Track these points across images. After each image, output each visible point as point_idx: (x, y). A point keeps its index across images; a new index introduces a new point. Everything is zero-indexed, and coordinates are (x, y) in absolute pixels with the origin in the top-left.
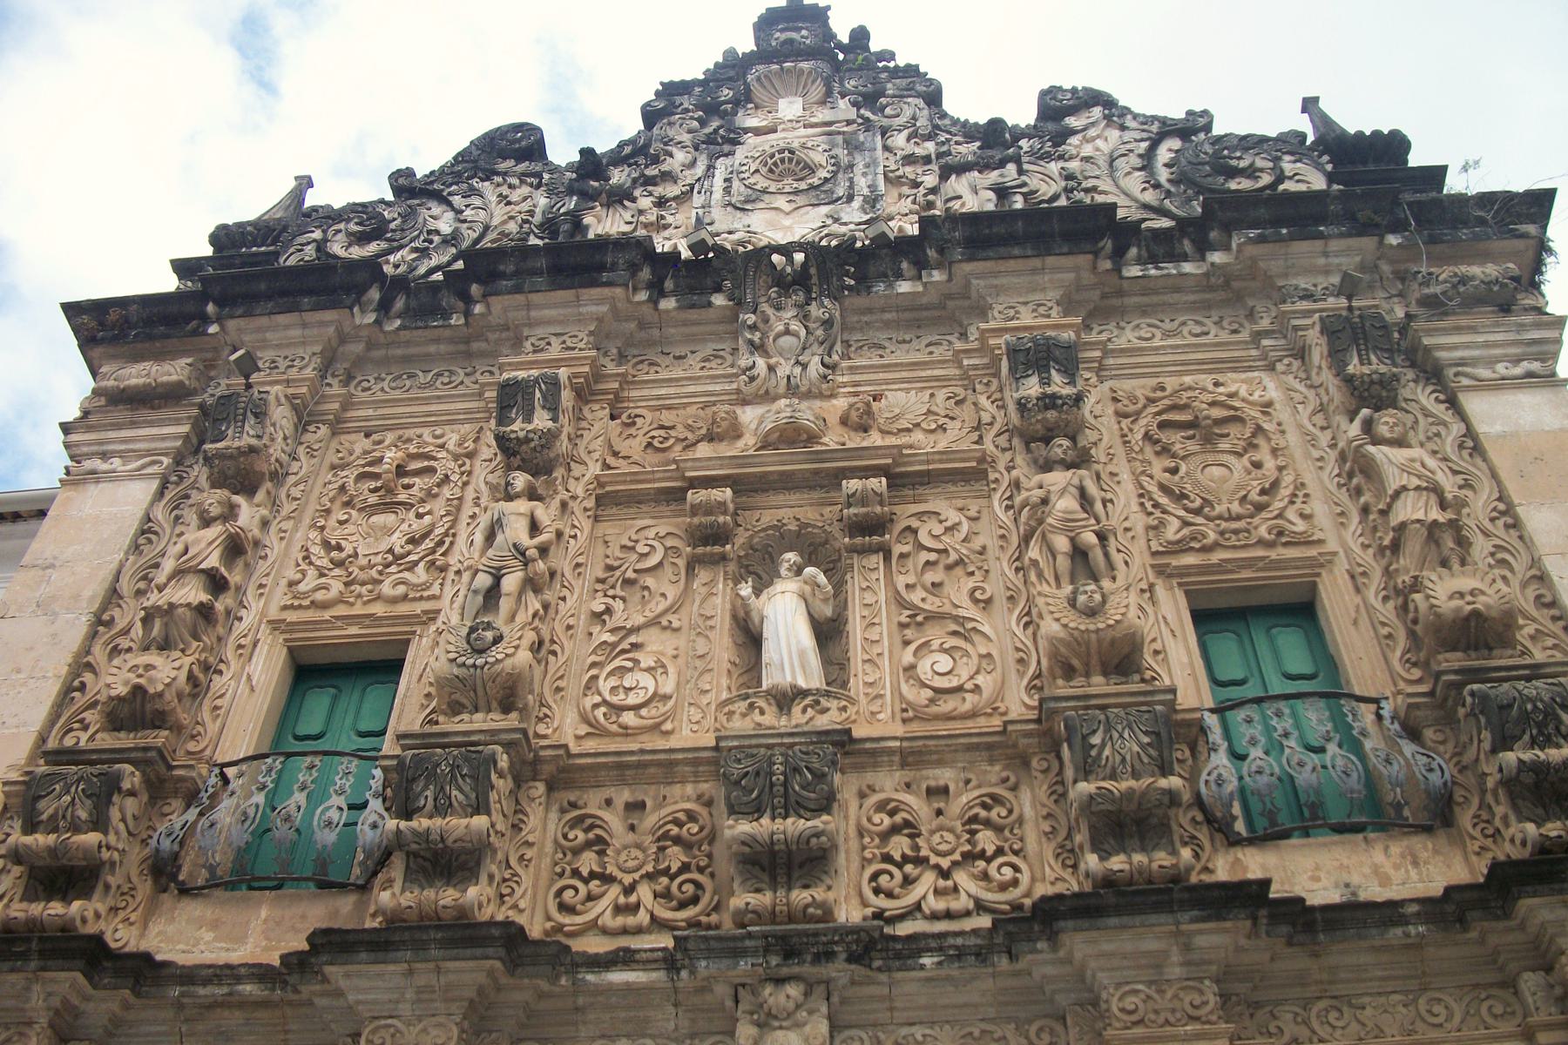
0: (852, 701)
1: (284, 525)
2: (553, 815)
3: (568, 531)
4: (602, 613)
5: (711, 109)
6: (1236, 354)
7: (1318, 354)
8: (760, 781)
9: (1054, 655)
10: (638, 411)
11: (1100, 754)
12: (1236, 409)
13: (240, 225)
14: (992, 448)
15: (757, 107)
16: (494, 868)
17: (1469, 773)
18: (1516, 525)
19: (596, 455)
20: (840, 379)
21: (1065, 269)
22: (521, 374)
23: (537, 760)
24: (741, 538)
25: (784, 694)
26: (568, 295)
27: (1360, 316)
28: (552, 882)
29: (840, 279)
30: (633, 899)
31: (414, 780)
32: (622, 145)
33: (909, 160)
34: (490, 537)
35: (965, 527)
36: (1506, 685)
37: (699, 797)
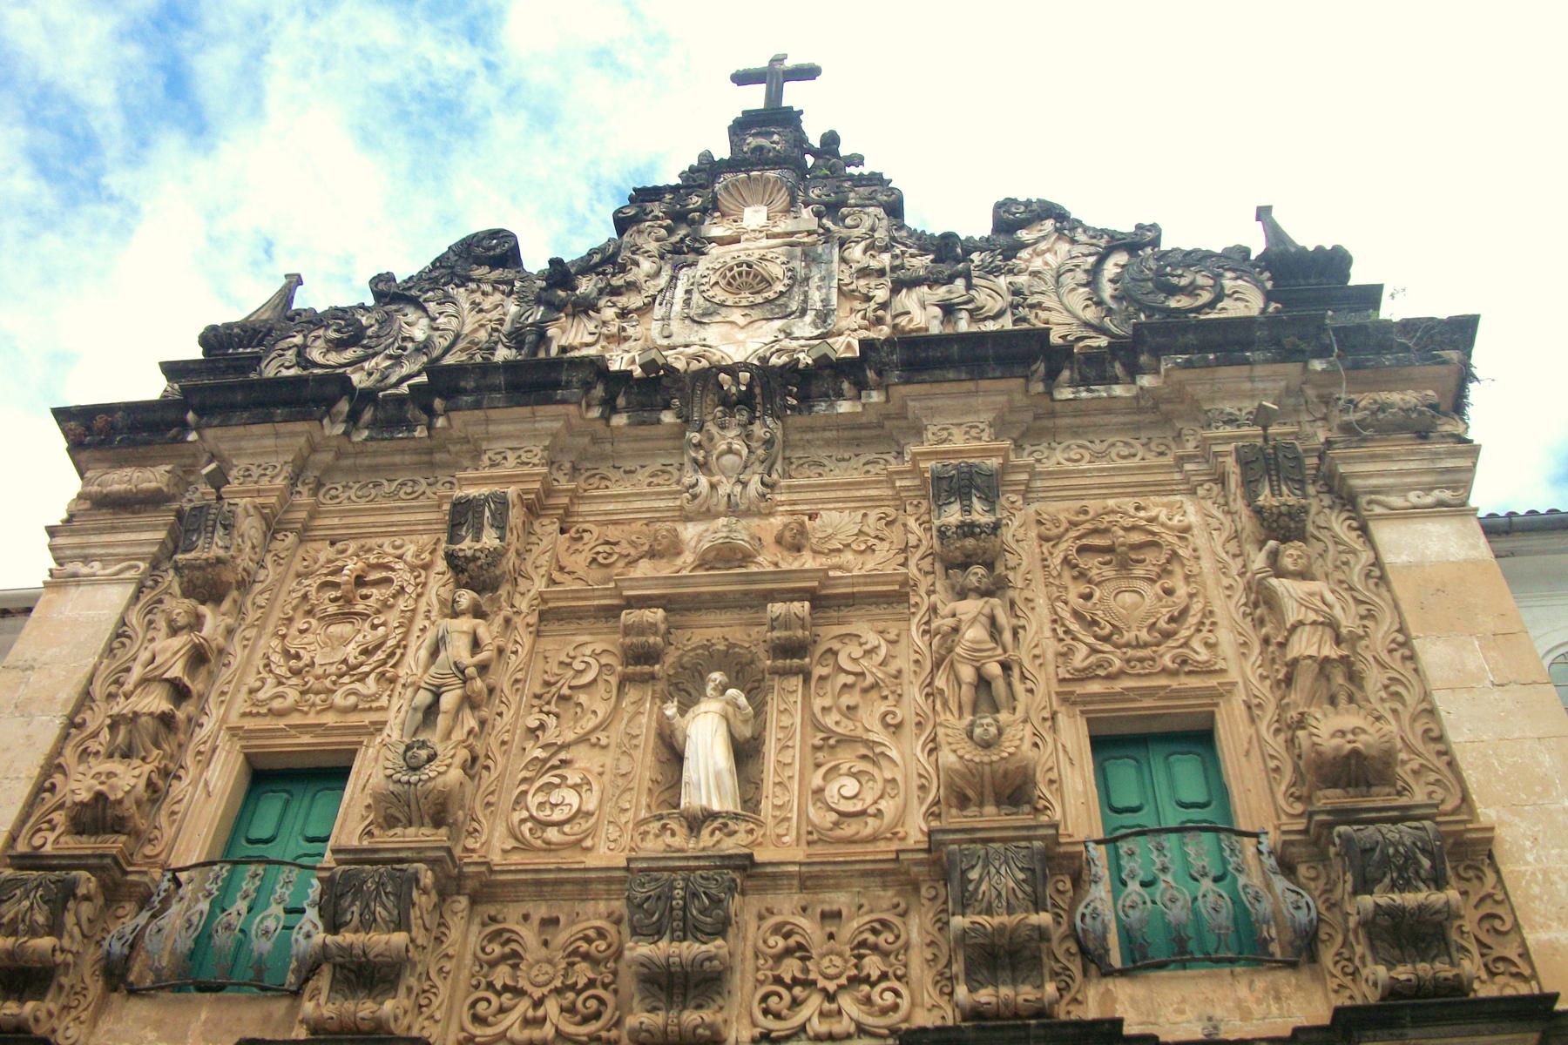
0: (760, 824)
1: (248, 634)
2: (475, 928)
3: (511, 647)
4: (537, 729)
5: (679, 217)
6: (1160, 477)
7: (1234, 480)
8: (661, 904)
9: (950, 786)
10: (586, 526)
11: (977, 889)
13: (228, 326)
14: (915, 571)
15: (723, 215)
16: (413, 981)
17: (1336, 910)
18: (1412, 658)
19: (542, 571)
20: (779, 498)
21: (999, 393)
22: (473, 492)
23: (462, 875)
24: (671, 657)
25: (695, 818)
26: (526, 411)
27: (1274, 447)
28: (469, 994)
29: (783, 399)
30: (540, 1012)
31: (342, 895)
32: (591, 254)
33: (864, 272)
34: (434, 653)
35: (883, 651)
36: (1371, 828)
37: (610, 915)
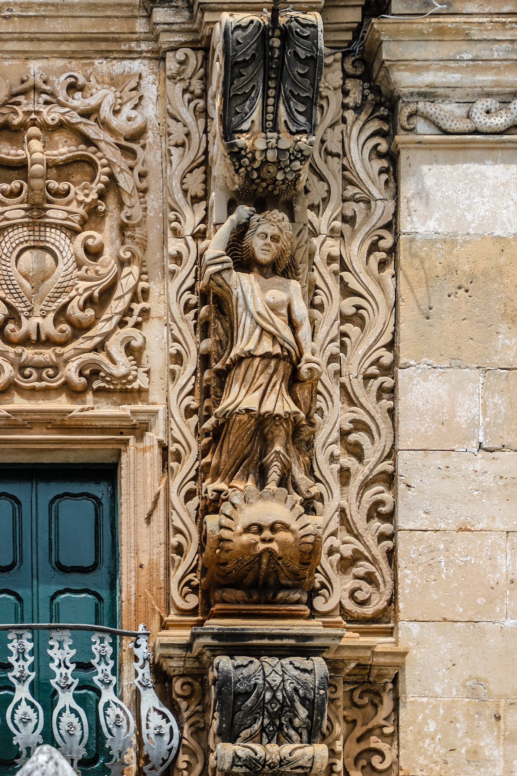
12: (88, 141)
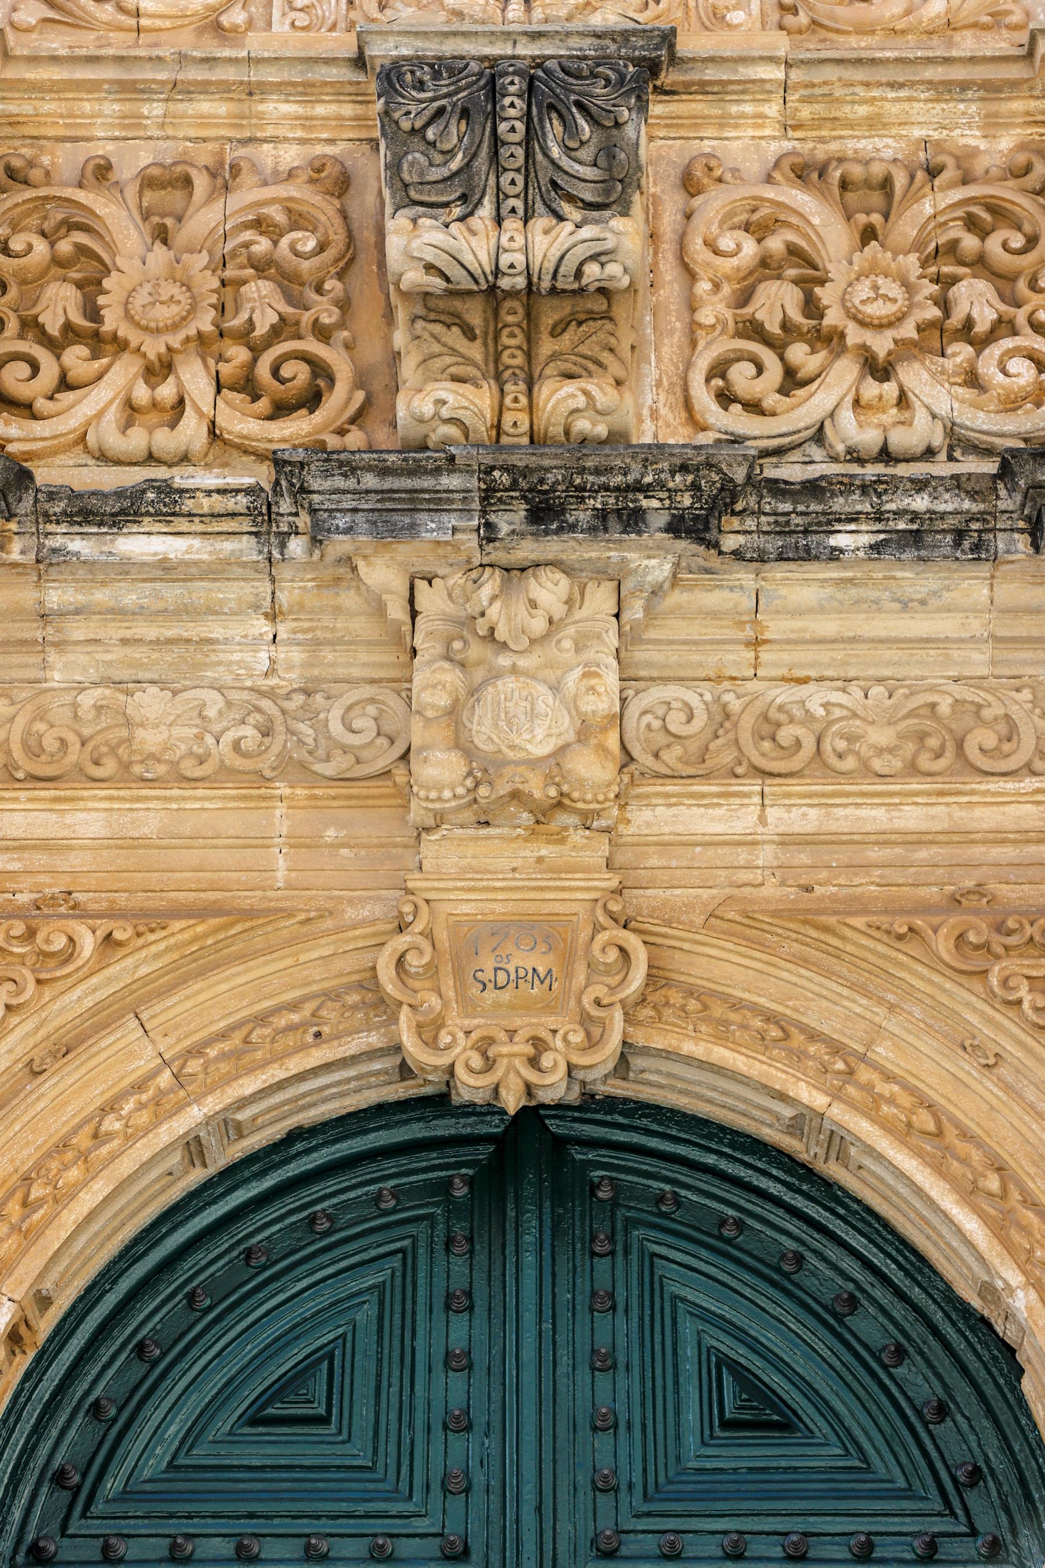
30: (167, 391)
